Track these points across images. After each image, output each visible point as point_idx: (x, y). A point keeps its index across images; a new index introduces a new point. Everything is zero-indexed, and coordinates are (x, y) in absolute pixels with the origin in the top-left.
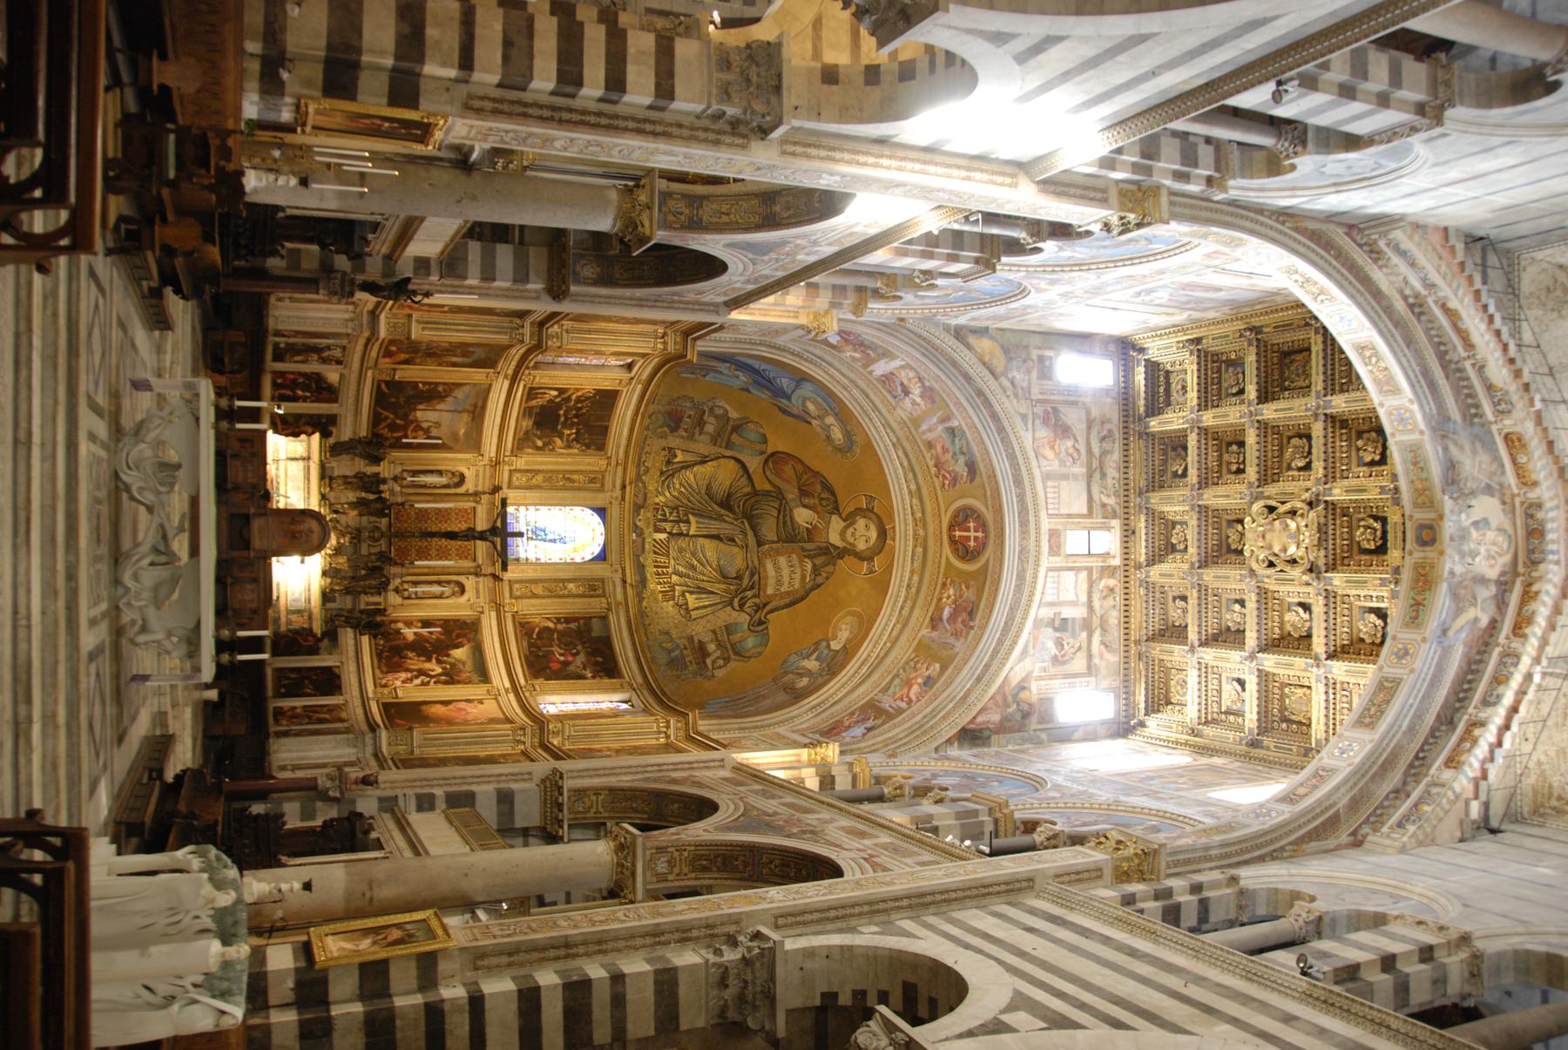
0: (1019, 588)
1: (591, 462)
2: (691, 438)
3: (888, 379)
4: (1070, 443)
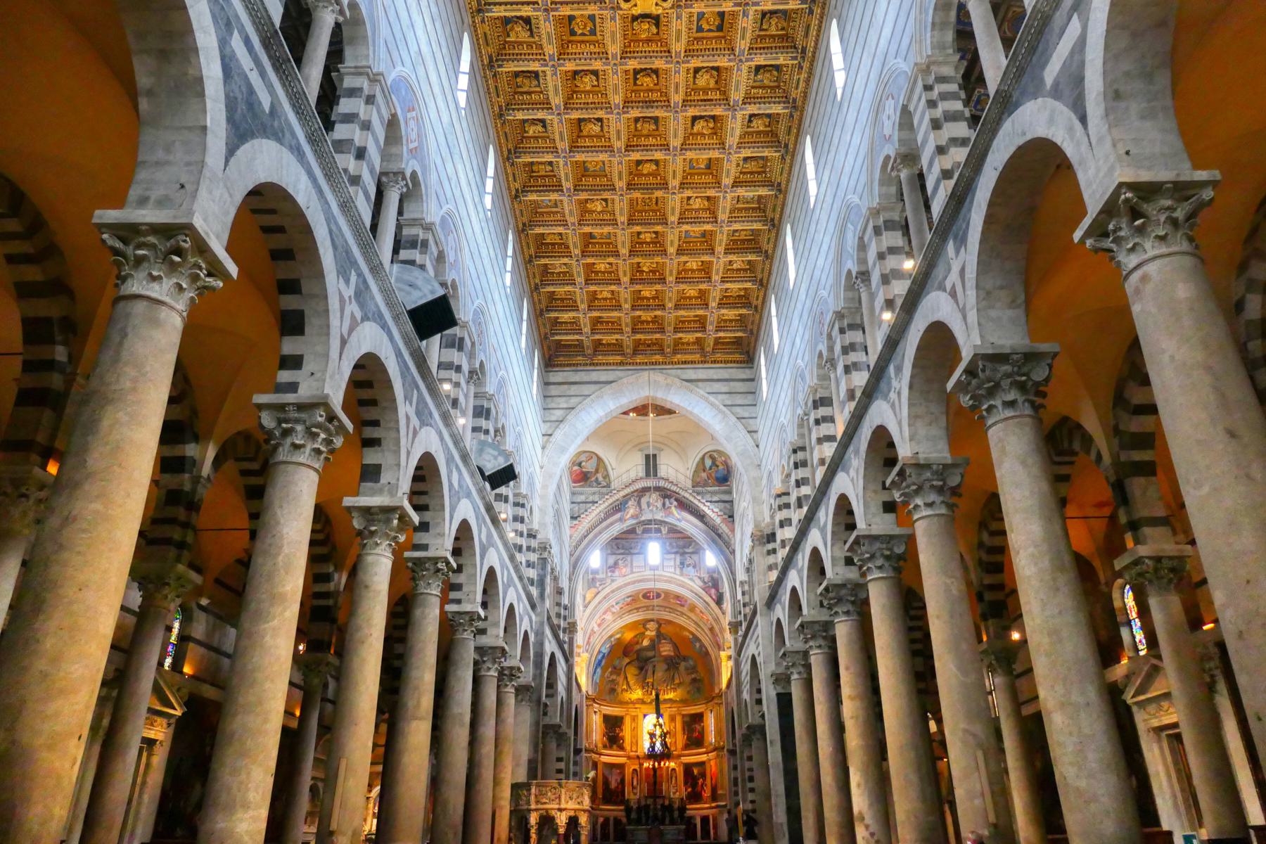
0: (670, 582)
1: (627, 721)
2: (618, 684)
3: (599, 625)
4: (620, 562)
